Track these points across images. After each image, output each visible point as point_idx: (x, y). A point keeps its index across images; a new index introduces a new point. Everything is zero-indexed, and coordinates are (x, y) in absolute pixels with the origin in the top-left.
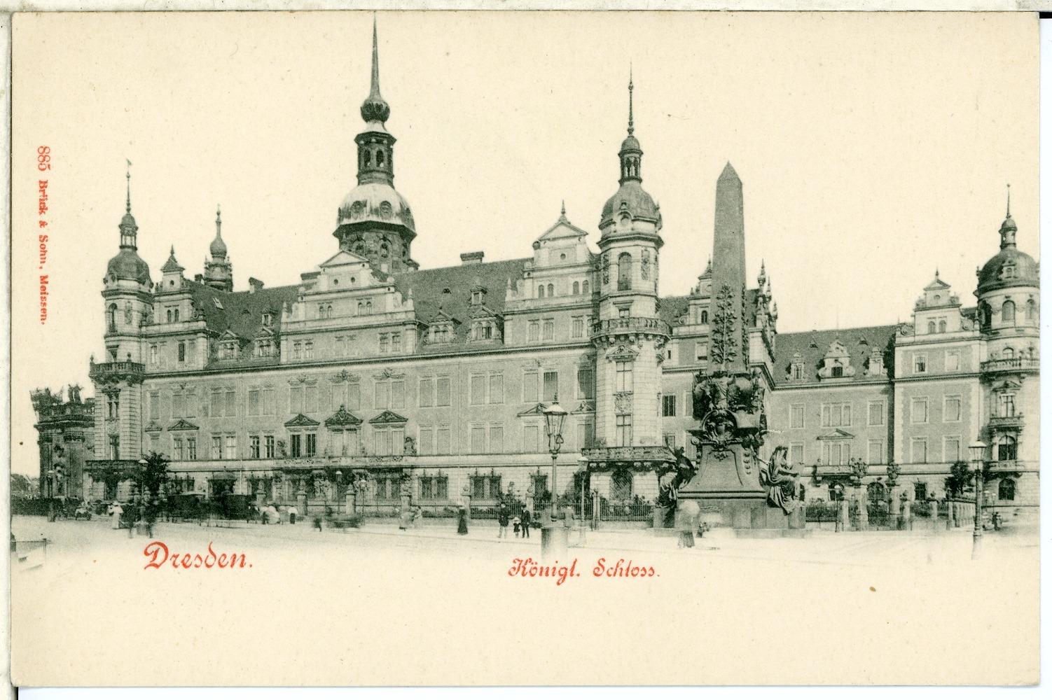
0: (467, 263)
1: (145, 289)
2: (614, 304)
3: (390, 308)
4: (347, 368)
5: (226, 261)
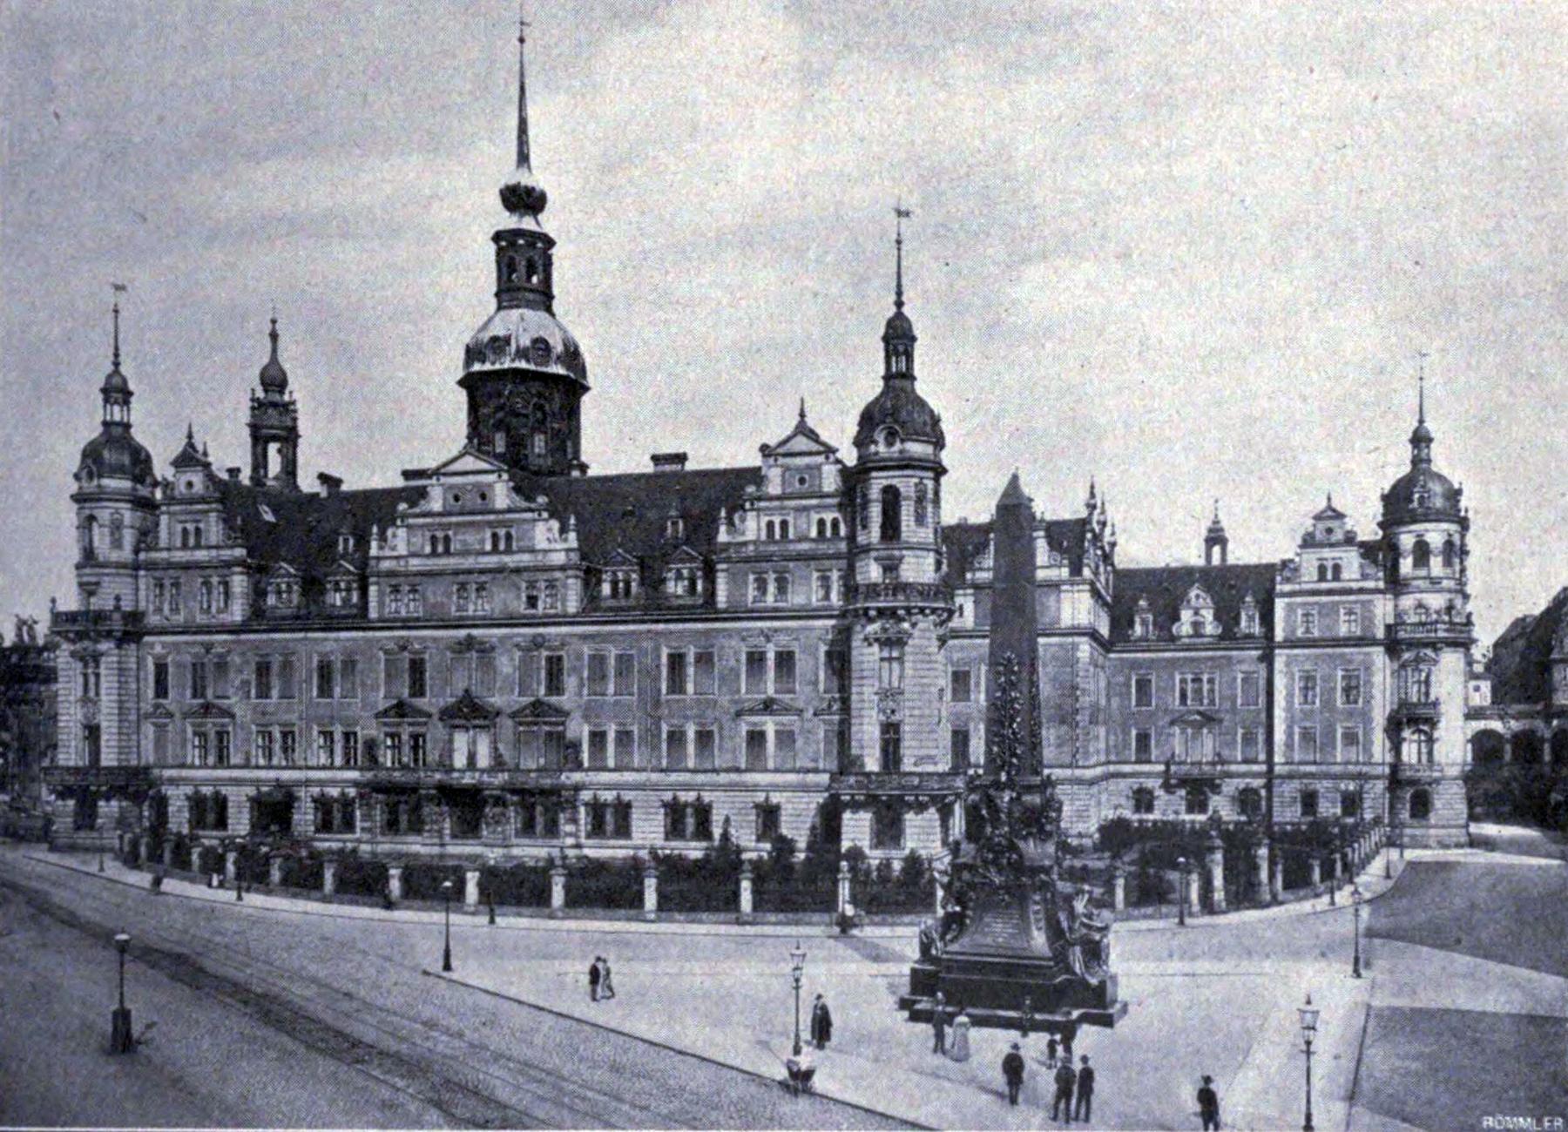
0: (660, 468)
1: (143, 491)
2: (876, 559)
5: (286, 398)
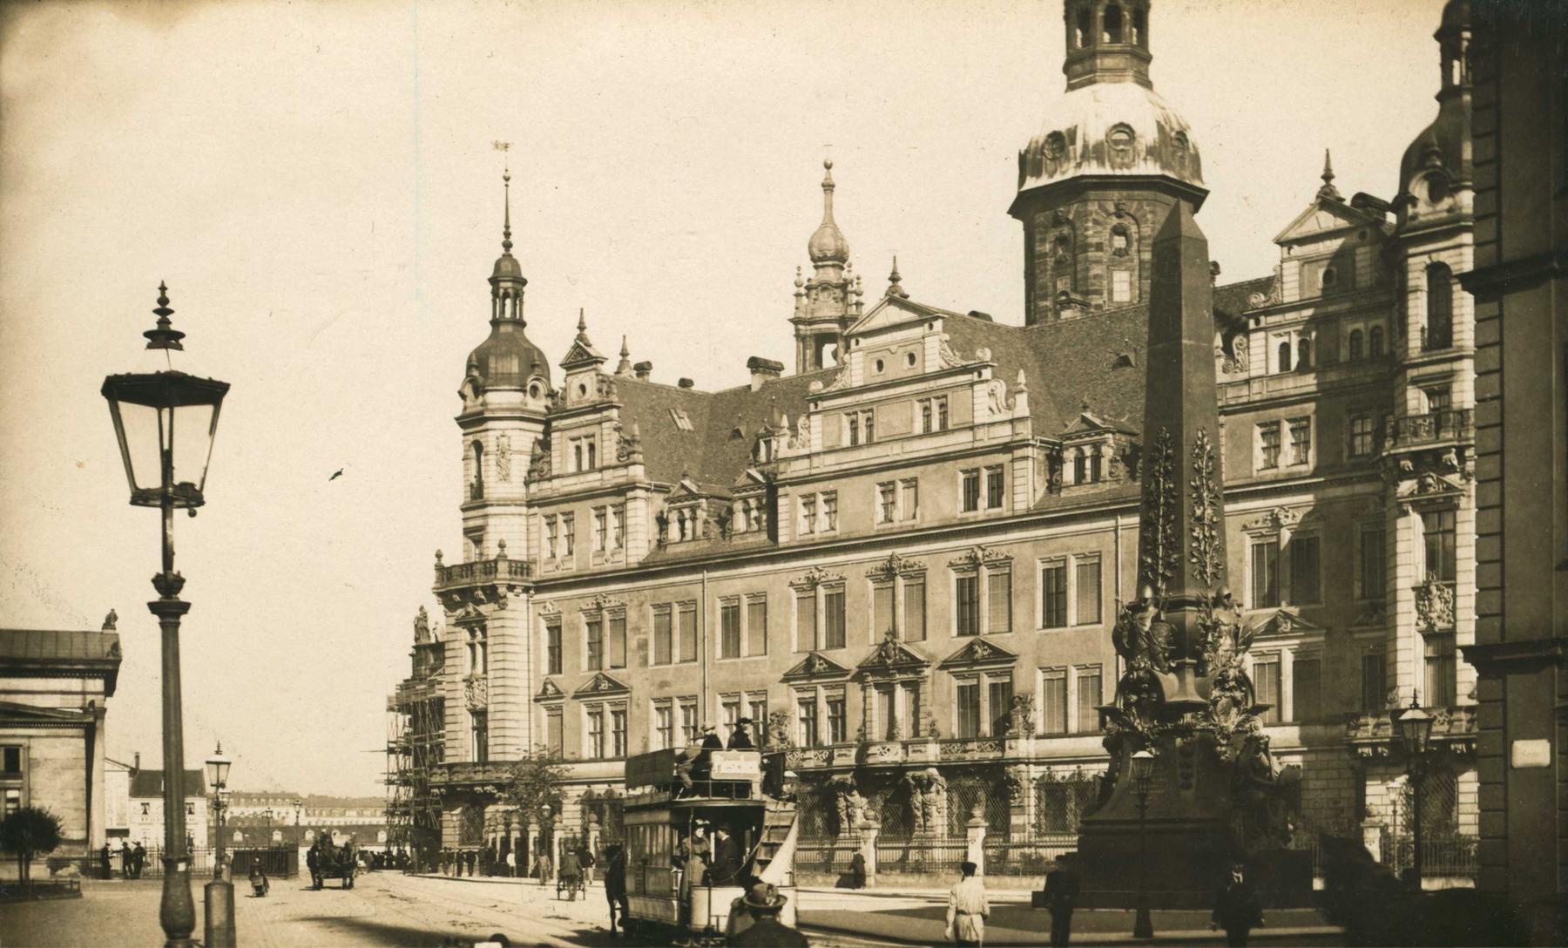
3: (982, 416)
4: (899, 551)
